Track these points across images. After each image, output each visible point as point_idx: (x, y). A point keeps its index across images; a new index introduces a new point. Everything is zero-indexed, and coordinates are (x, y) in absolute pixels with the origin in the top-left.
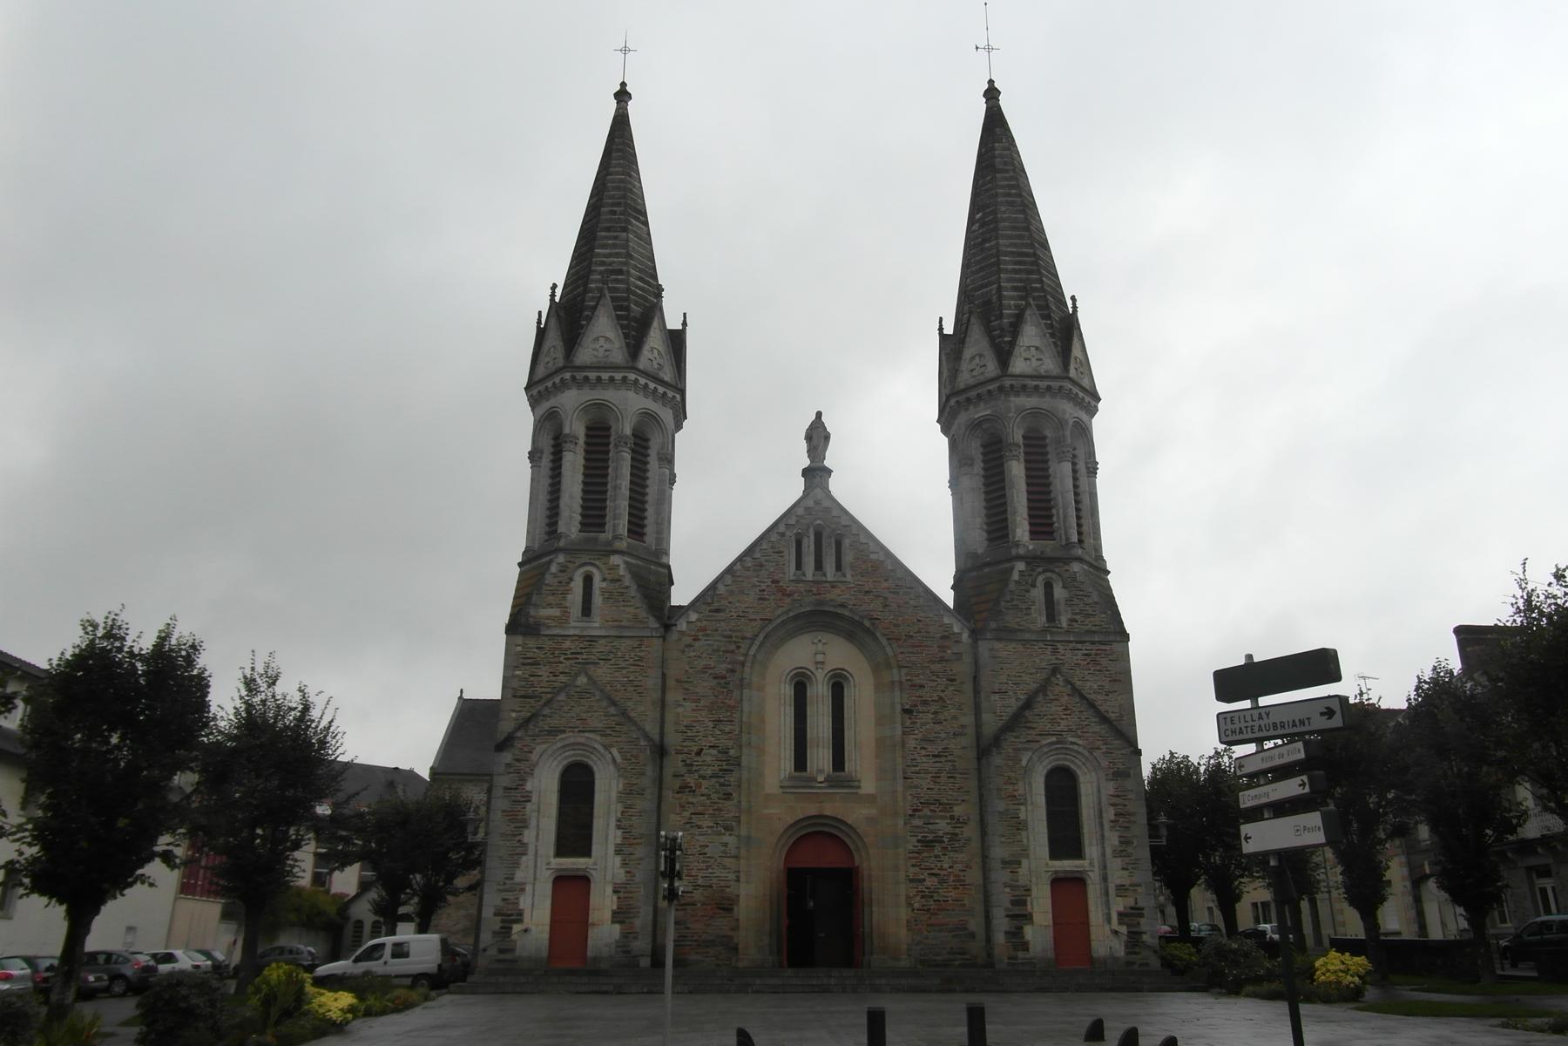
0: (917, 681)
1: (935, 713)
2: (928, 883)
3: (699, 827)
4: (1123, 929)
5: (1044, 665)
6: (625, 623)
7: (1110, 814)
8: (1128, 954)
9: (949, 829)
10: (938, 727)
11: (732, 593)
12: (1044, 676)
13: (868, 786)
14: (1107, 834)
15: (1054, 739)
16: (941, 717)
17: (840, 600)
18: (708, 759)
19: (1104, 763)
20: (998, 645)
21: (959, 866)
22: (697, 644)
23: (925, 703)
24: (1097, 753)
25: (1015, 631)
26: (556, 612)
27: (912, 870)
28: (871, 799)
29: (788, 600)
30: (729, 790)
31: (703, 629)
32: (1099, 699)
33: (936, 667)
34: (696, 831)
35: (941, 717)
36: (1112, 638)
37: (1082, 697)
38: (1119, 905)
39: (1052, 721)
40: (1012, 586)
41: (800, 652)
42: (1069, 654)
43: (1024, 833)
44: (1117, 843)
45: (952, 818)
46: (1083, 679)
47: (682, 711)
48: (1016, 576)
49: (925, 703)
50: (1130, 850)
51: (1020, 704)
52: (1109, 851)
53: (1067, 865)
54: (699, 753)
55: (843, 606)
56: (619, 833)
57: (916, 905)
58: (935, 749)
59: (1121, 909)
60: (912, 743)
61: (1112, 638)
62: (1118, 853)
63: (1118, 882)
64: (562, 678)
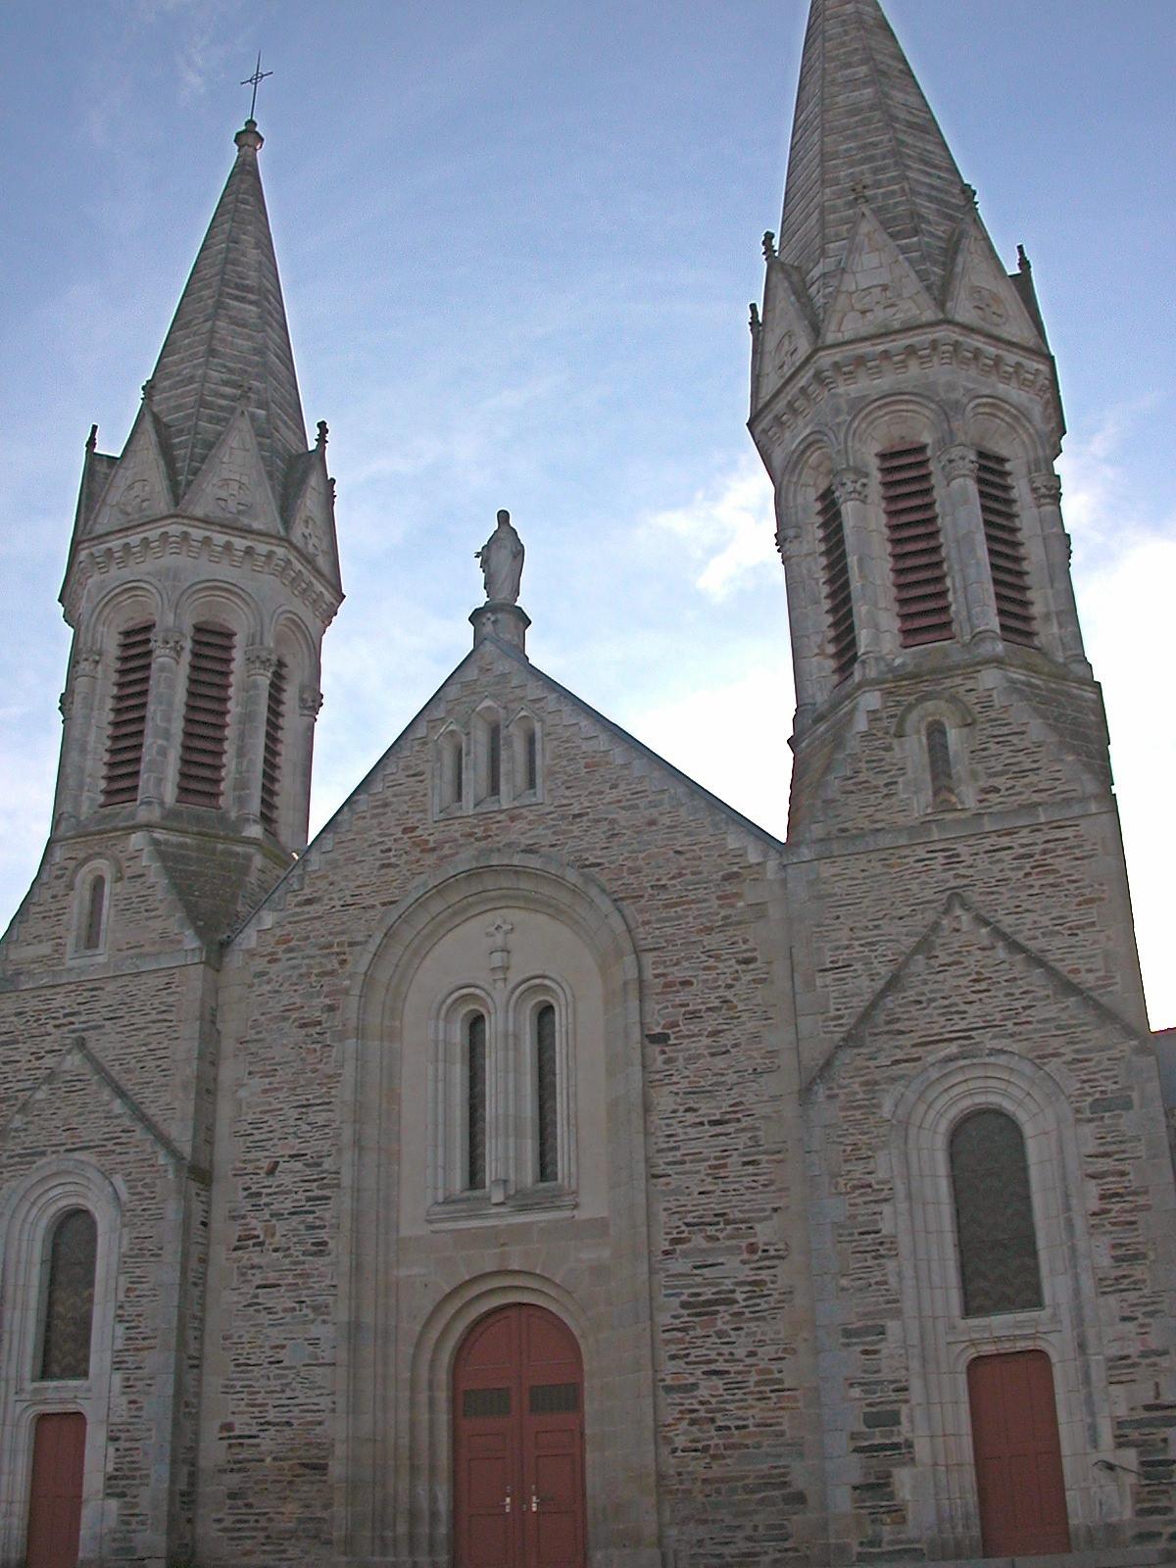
0: (677, 974)
1: (715, 1033)
2: (703, 1392)
3: (269, 1310)
4: (1130, 1457)
5: (928, 894)
6: (147, 949)
7: (1090, 1196)
8: (1141, 1513)
9: (746, 1273)
10: (720, 1063)
11: (334, 865)
12: (930, 916)
13: (593, 1205)
14: (1082, 1245)
15: (953, 1049)
16: (726, 1040)
17: (525, 841)
18: (287, 1180)
19: (1073, 1086)
20: (826, 870)
21: (770, 1351)
22: (275, 968)
23: (694, 1015)
24: (1052, 1066)
25: (862, 834)
26: (45, 949)
27: (672, 1366)
28: (600, 1227)
29: (430, 859)
30: (323, 1235)
31: (285, 940)
32: (1054, 948)
33: (712, 941)
34: (264, 1318)
35: (726, 1040)
36: (1077, 810)
37: (1014, 947)
38: (1119, 1403)
39: (948, 1012)
40: (854, 745)
41: (463, 955)
42: (983, 862)
43: (891, 1265)
44: (1106, 1262)
45: (752, 1248)
46: (1018, 911)
47: (242, 1091)
48: (861, 724)
49: (694, 1015)
50: (1138, 1271)
51: (879, 985)
52: (1087, 1283)
53: (1002, 1327)
54: (271, 1172)
55: (530, 850)
56: (120, 1329)
57: (681, 1441)
58: (708, 1109)
59: (1122, 1411)
60: (664, 1100)
61: (1077, 810)
62: (1107, 1286)
63: (1114, 1350)
64: (49, 1061)
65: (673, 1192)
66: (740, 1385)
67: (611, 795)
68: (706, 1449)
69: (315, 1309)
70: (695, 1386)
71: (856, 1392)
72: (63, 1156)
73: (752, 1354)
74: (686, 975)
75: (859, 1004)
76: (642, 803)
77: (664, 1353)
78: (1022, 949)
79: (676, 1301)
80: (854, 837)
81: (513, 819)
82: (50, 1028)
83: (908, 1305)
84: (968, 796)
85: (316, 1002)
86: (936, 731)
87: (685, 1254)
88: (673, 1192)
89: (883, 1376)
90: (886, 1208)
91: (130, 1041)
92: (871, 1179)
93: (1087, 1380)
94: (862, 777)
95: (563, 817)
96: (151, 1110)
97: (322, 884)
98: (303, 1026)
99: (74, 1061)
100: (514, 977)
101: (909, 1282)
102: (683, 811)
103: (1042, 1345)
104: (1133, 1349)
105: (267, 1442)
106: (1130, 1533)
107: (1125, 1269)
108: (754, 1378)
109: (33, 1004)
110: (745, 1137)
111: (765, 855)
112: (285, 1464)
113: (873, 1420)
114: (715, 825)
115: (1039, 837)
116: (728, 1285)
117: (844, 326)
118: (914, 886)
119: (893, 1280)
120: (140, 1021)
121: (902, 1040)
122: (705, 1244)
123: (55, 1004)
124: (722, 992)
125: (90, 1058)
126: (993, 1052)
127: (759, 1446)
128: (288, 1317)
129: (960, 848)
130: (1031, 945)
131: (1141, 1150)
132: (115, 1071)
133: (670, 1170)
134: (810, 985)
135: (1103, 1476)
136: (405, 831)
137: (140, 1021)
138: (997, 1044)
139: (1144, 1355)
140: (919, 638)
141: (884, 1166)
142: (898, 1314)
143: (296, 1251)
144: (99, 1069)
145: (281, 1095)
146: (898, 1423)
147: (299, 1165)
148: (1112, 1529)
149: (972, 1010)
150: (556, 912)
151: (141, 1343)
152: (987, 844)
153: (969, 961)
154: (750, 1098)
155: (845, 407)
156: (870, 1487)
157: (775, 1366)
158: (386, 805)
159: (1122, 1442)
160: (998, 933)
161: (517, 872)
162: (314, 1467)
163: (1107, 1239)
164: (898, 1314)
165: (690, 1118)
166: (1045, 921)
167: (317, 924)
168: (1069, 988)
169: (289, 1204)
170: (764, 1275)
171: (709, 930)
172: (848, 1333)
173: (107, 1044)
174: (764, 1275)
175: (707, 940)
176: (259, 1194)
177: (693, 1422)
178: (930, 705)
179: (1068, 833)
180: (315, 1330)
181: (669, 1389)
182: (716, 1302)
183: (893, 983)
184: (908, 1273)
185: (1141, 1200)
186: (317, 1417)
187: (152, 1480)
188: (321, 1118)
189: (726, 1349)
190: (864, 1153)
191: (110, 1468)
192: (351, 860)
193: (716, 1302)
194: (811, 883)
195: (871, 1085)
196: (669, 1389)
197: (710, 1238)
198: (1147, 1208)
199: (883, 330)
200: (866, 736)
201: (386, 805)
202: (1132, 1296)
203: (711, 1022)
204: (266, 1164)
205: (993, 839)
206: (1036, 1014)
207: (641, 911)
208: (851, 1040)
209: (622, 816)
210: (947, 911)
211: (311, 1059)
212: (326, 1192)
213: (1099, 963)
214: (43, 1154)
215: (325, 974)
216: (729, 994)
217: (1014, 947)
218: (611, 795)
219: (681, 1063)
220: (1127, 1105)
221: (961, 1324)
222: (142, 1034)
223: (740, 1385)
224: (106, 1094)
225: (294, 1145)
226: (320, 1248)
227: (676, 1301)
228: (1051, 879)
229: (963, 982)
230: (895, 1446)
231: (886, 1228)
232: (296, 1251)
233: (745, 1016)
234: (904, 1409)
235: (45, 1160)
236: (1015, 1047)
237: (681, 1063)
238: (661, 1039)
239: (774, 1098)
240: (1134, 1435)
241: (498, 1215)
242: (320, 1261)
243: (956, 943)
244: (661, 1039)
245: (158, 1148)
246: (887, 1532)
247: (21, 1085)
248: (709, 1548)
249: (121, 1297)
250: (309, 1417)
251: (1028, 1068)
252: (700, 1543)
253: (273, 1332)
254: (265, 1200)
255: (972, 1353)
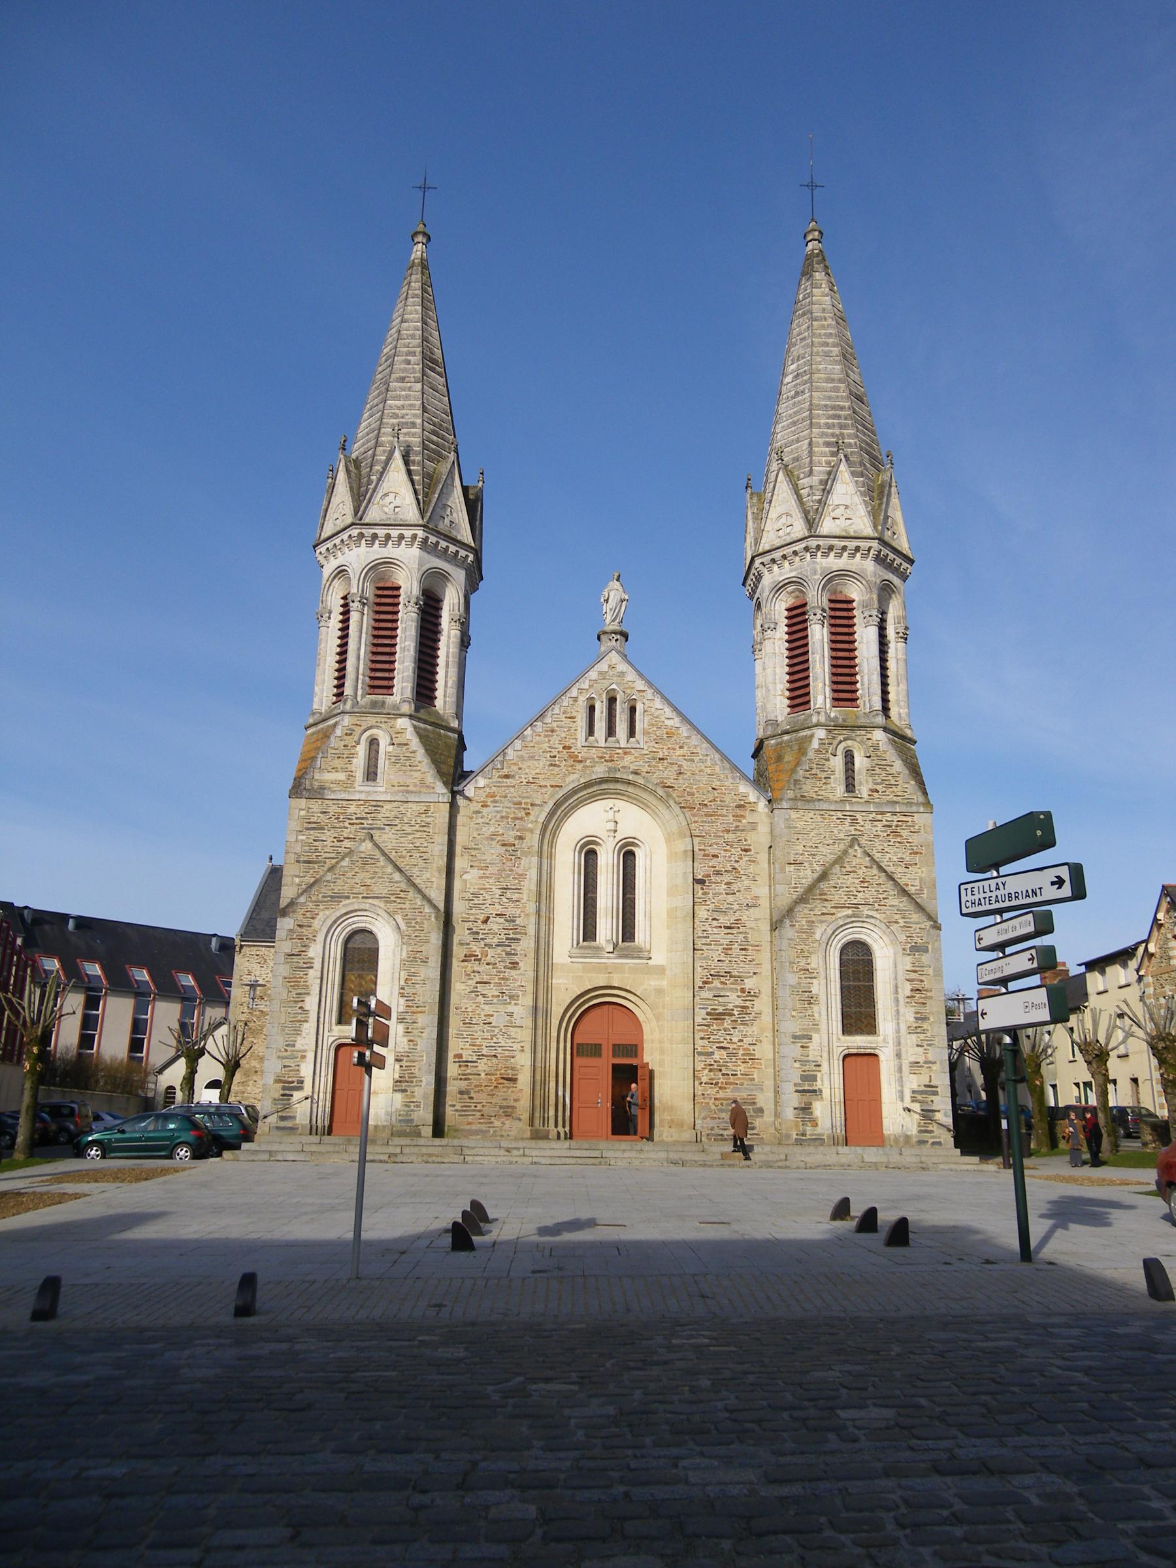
0: (711, 850)
1: (727, 884)
2: (716, 1056)
3: (484, 995)
4: (916, 1107)
5: (842, 836)
6: (411, 788)
7: (906, 989)
8: (921, 1131)
9: (739, 1002)
10: (730, 898)
11: (522, 758)
12: (842, 847)
13: (659, 957)
14: (902, 1010)
15: (850, 912)
16: (734, 887)
17: (633, 767)
18: (495, 927)
19: (902, 938)
20: (794, 815)
21: (747, 1040)
22: (485, 810)
23: (718, 873)
24: (894, 927)
25: (812, 800)
26: (341, 776)
27: (701, 1043)
28: (661, 970)
29: (579, 766)
30: (516, 959)
31: (493, 795)
32: (898, 872)
33: (730, 837)
34: (481, 999)
35: (734, 887)
36: (914, 809)
37: (881, 869)
38: (913, 1082)
39: (849, 894)
40: (811, 754)
41: (590, 820)
42: (868, 825)
43: (816, 1008)
44: (912, 1019)
45: (743, 991)
46: (882, 851)
47: (467, 878)
48: (815, 744)
49: (718, 873)
50: (926, 1026)
51: (816, 875)
52: (903, 1027)
53: (859, 1042)
54: (485, 921)
55: (636, 773)
56: (402, 1001)
57: (704, 1079)
58: (724, 920)
59: (915, 1087)
60: (702, 913)
61: (914, 809)
62: (914, 1030)
63: (913, 1059)
64: (347, 843)
65: (705, 958)
66: (735, 1055)
67: (680, 752)
68: (717, 1084)
69: (511, 997)
70: (713, 1053)
71: (797, 1065)
72: (361, 900)
73: (741, 1041)
74: (716, 852)
75: (807, 882)
76: (696, 759)
77: (697, 1037)
78: (885, 871)
79: (704, 1012)
80: (808, 801)
81: (625, 753)
82: (346, 824)
83: (823, 1027)
84: (863, 790)
85: (511, 833)
86: (849, 757)
87: (709, 989)
88: (705, 958)
89: (810, 1058)
90: (814, 981)
91: (402, 840)
92: (808, 967)
93: (900, 1070)
94: (814, 772)
95: (654, 758)
96: (417, 881)
97: (515, 768)
98: (503, 845)
99: (367, 846)
100: (619, 836)
101: (824, 1017)
102: (717, 768)
103: (877, 1052)
104: (921, 1060)
105: (482, 1066)
106: (915, 1140)
107: (920, 1023)
108: (741, 1052)
109: (333, 809)
110: (741, 936)
111: (758, 799)
112: (493, 1078)
113: (804, 1078)
114: (734, 778)
115: (895, 818)
116: (730, 1006)
117: (827, 526)
118: (836, 832)
119: (816, 1015)
120: (409, 830)
121: (827, 904)
122: (719, 985)
123: (349, 811)
124: (733, 863)
125: (376, 845)
126: (868, 916)
127: (742, 1084)
128: (495, 1000)
129: (858, 816)
130: (889, 869)
131: (931, 972)
132: (393, 855)
133: (704, 947)
134: (783, 870)
135: (905, 1114)
136: (564, 748)
137: (406, 827)
138: (870, 913)
139: (926, 1062)
140: (841, 703)
141: (815, 962)
142: (818, 1031)
143: (500, 966)
144: (384, 854)
145: (491, 881)
146: (816, 1080)
147: (502, 920)
148: (908, 1138)
149: (860, 895)
150: (644, 805)
151: (415, 1009)
152: (871, 816)
153: (860, 872)
154: (745, 918)
155: (819, 571)
156: (803, 1109)
157: (751, 1048)
158: (553, 731)
159: (914, 1100)
160: (873, 860)
161: (629, 783)
162: (508, 1079)
163: (913, 1009)
164: (818, 1031)
165: (715, 923)
166: (895, 859)
167: (512, 790)
168: (904, 892)
169: (496, 940)
170: (748, 1004)
171: (728, 831)
172: (795, 1037)
173: (387, 839)
174: (748, 1004)
175: (726, 836)
176: (478, 933)
177: (711, 1070)
178: (849, 743)
179: (909, 819)
180: (510, 1008)
181: (700, 1054)
182: (724, 1014)
183: (824, 876)
184: (824, 1012)
185: (929, 994)
186: (511, 1054)
187: (423, 1084)
188: (515, 897)
189: (728, 1037)
190: (806, 954)
191: (397, 1076)
192: (532, 758)
193: (724, 1014)
194: (787, 820)
195: (811, 923)
196: (700, 1054)
197: (722, 983)
198: (931, 998)
199: (844, 534)
200: (818, 751)
201: (553, 731)
202: (922, 1036)
203: (727, 878)
204: (482, 917)
205: (874, 815)
206: (889, 902)
207: (694, 815)
208: (802, 900)
209: (684, 763)
210: (851, 846)
211: (508, 864)
212: (518, 936)
213: (917, 883)
214: (348, 897)
215: (517, 818)
216: (736, 865)
217: (881, 869)
218: (680, 752)
219: (711, 895)
220: (926, 951)
221: (843, 1038)
222: (410, 837)
223: (735, 1055)
224: (390, 869)
225: (499, 909)
226: (514, 965)
227: (704, 1012)
228: (899, 839)
229: (857, 881)
230: (815, 1091)
231: (815, 991)
232: (500, 966)
233: (744, 878)
234: (819, 1075)
235: (347, 901)
236: (878, 916)
237: (711, 895)
238: (701, 882)
239: (756, 920)
240: (919, 1097)
241: (609, 958)
242: (513, 972)
243: (855, 862)
244: (701, 882)
245: (425, 903)
246: (809, 1130)
247: (327, 855)
248: (717, 1131)
249: (402, 983)
250: (507, 1053)
251: (884, 927)
252: (712, 1129)
253: (487, 1007)
254: (481, 936)
255: (846, 1052)
